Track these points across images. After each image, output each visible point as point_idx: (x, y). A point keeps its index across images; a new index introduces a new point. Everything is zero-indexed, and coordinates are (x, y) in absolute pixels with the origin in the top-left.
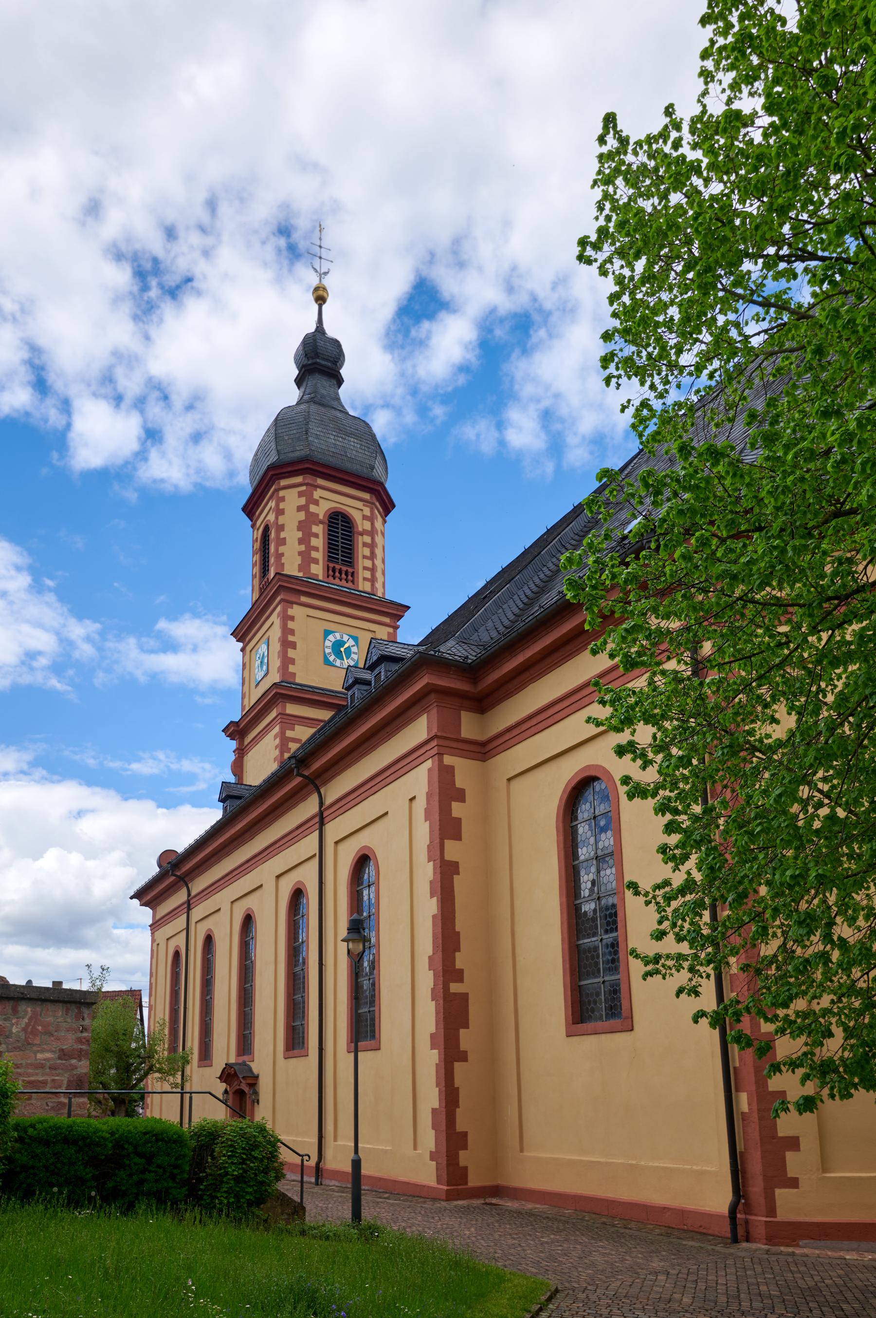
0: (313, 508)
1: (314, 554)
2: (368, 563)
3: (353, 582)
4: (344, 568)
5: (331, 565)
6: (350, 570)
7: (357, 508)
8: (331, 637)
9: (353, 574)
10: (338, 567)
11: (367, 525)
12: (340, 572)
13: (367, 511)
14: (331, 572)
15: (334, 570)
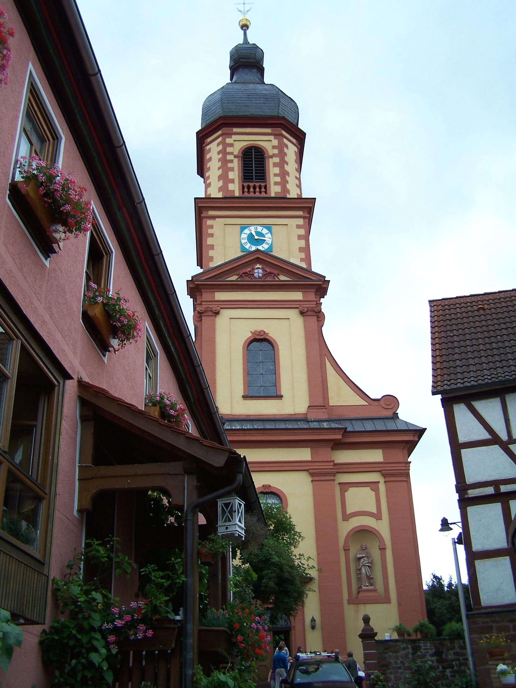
0: (229, 149)
3: (266, 192)
4: (257, 184)
5: (246, 184)
7: (267, 142)
9: (265, 187)
10: (252, 184)
11: (276, 151)
13: (275, 142)
14: (246, 190)
15: (249, 187)
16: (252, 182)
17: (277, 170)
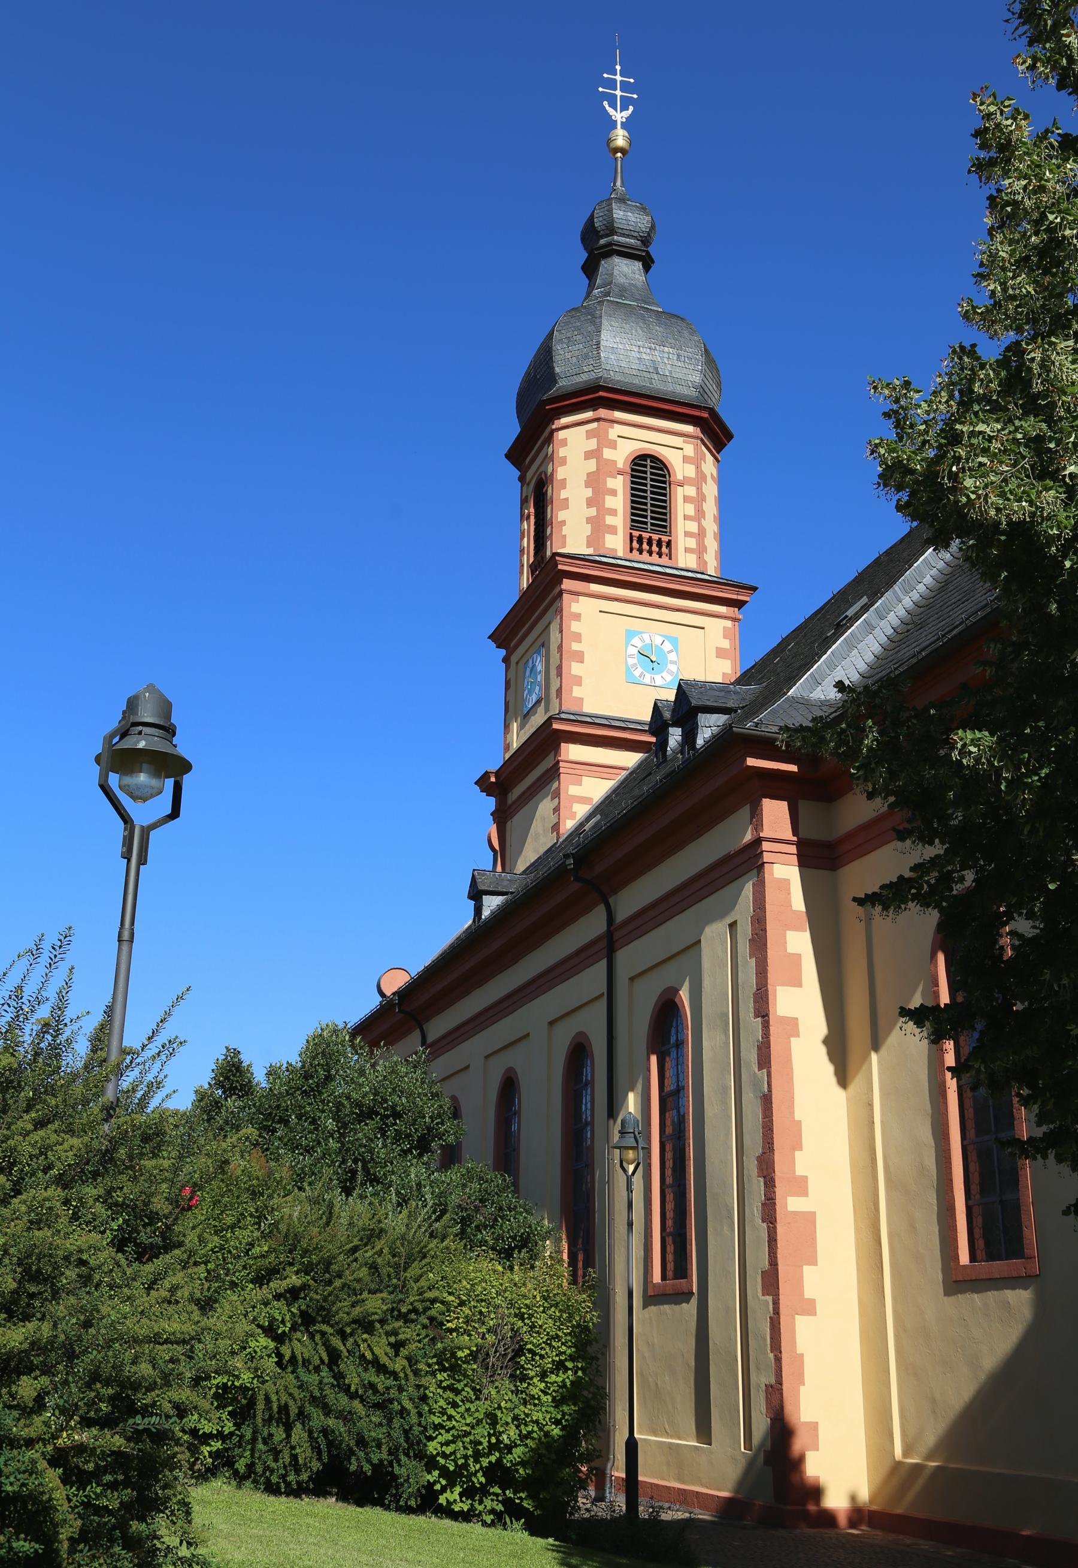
1: (609, 520)
2: (693, 527)
4: (655, 537)
5: (636, 533)
6: (665, 539)
8: (636, 641)
9: (669, 544)
10: (646, 535)
11: (690, 471)
12: (650, 542)
13: (689, 449)
14: (635, 545)
15: (640, 540)
16: (645, 530)
17: (690, 509)
